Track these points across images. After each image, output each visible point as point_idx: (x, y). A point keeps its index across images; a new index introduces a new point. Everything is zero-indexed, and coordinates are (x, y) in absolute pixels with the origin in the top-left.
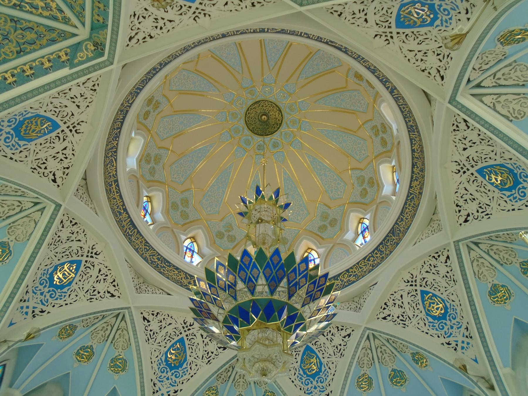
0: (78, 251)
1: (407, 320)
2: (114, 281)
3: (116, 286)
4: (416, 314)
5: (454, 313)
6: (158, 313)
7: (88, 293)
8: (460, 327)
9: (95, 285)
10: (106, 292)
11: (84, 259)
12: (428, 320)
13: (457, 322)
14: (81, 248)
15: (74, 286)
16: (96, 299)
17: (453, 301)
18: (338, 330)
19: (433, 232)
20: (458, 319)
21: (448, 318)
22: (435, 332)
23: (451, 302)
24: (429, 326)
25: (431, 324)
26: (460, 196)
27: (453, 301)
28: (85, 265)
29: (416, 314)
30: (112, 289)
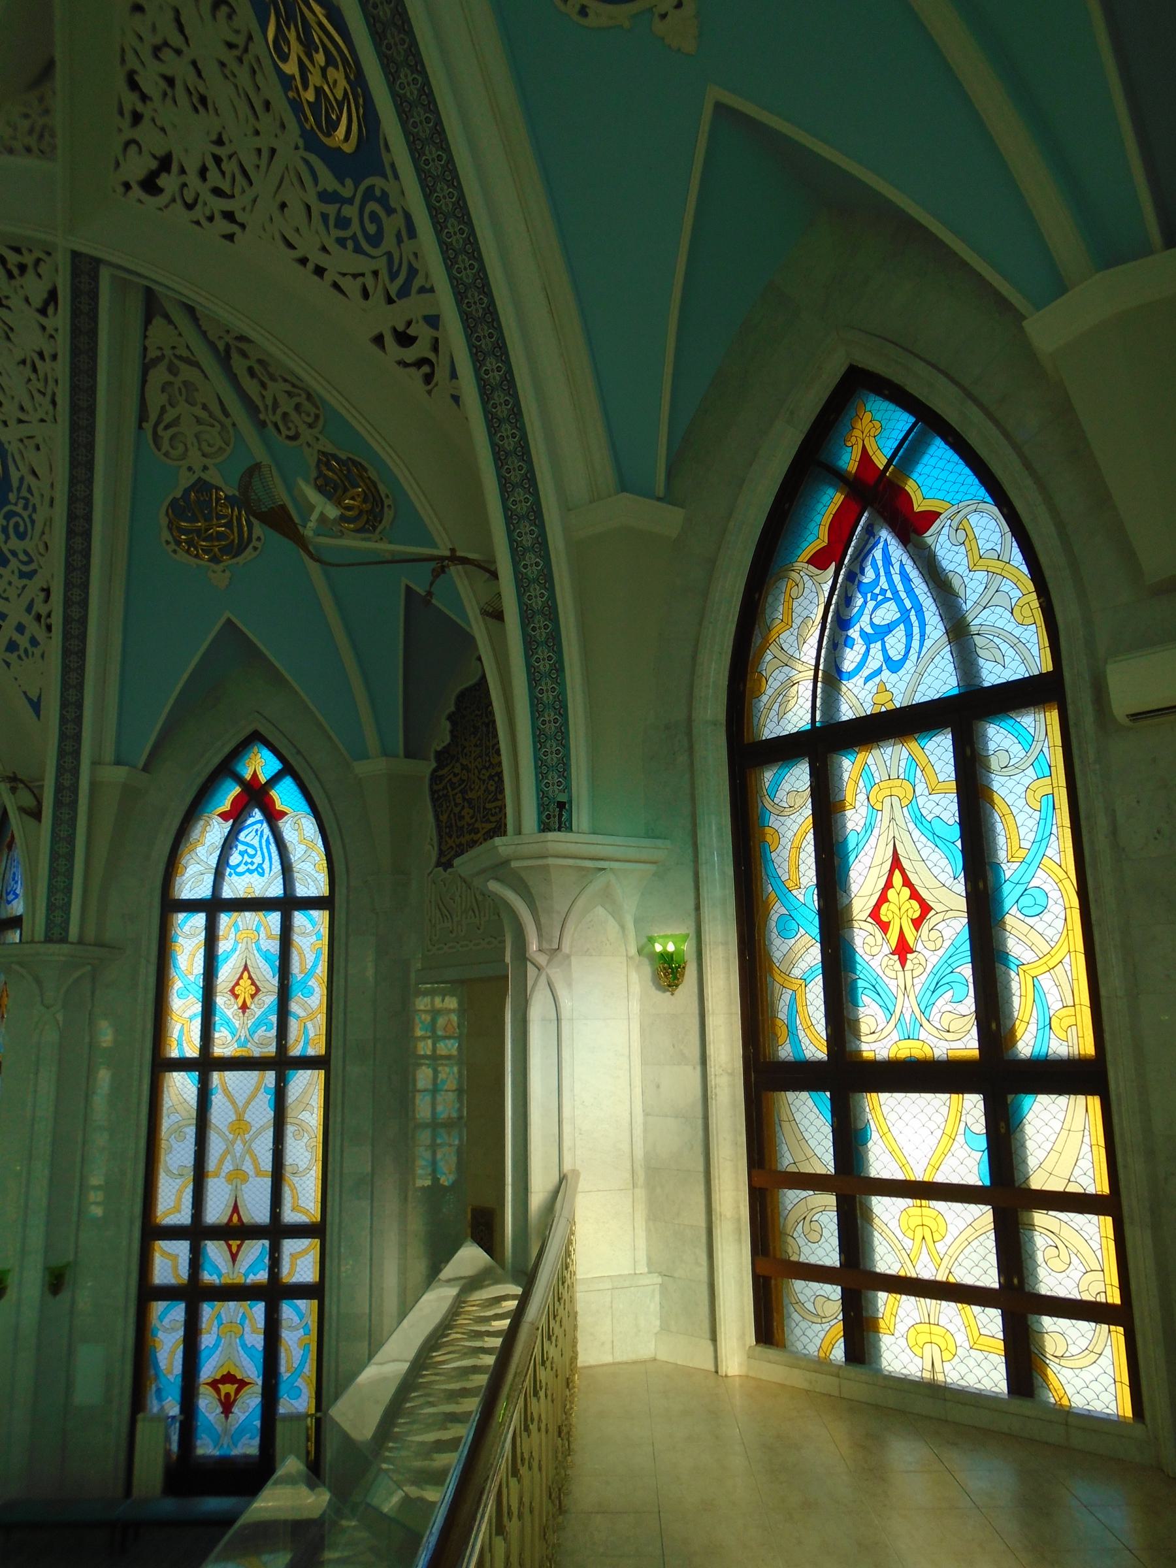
5: (25, 514)
8: (30, 575)
13: (26, 553)
23: (24, 470)
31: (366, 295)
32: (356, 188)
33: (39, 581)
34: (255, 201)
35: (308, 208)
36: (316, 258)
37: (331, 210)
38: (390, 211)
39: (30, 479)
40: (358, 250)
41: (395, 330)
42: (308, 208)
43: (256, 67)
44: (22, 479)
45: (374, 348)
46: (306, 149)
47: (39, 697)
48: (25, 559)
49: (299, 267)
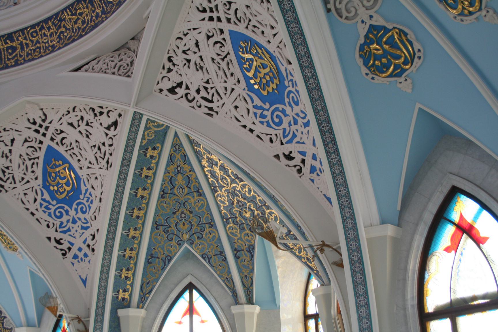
1: (9, 181)
4: (26, 178)
5: (87, 204)
8: (86, 228)
12: (42, 195)
13: (85, 219)
17: (93, 187)
19: (116, 70)
20: (87, 216)
21: (74, 206)
22: (46, 217)
23: (89, 186)
24: (41, 205)
25: (45, 204)
26: (182, 48)
27: (93, 187)
29: (26, 178)
31: (271, 141)
32: (270, 107)
33: (90, 231)
34: (223, 104)
35: (248, 110)
36: (250, 126)
37: (259, 112)
38: (286, 115)
39: (91, 190)
40: (269, 125)
41: (284, 154)
42: (248, 110)
43: (230, 62)
45: (275, 160)
46: (248, 90)
47: (86, 279)
48: (85, 222)
49: (243, 129)
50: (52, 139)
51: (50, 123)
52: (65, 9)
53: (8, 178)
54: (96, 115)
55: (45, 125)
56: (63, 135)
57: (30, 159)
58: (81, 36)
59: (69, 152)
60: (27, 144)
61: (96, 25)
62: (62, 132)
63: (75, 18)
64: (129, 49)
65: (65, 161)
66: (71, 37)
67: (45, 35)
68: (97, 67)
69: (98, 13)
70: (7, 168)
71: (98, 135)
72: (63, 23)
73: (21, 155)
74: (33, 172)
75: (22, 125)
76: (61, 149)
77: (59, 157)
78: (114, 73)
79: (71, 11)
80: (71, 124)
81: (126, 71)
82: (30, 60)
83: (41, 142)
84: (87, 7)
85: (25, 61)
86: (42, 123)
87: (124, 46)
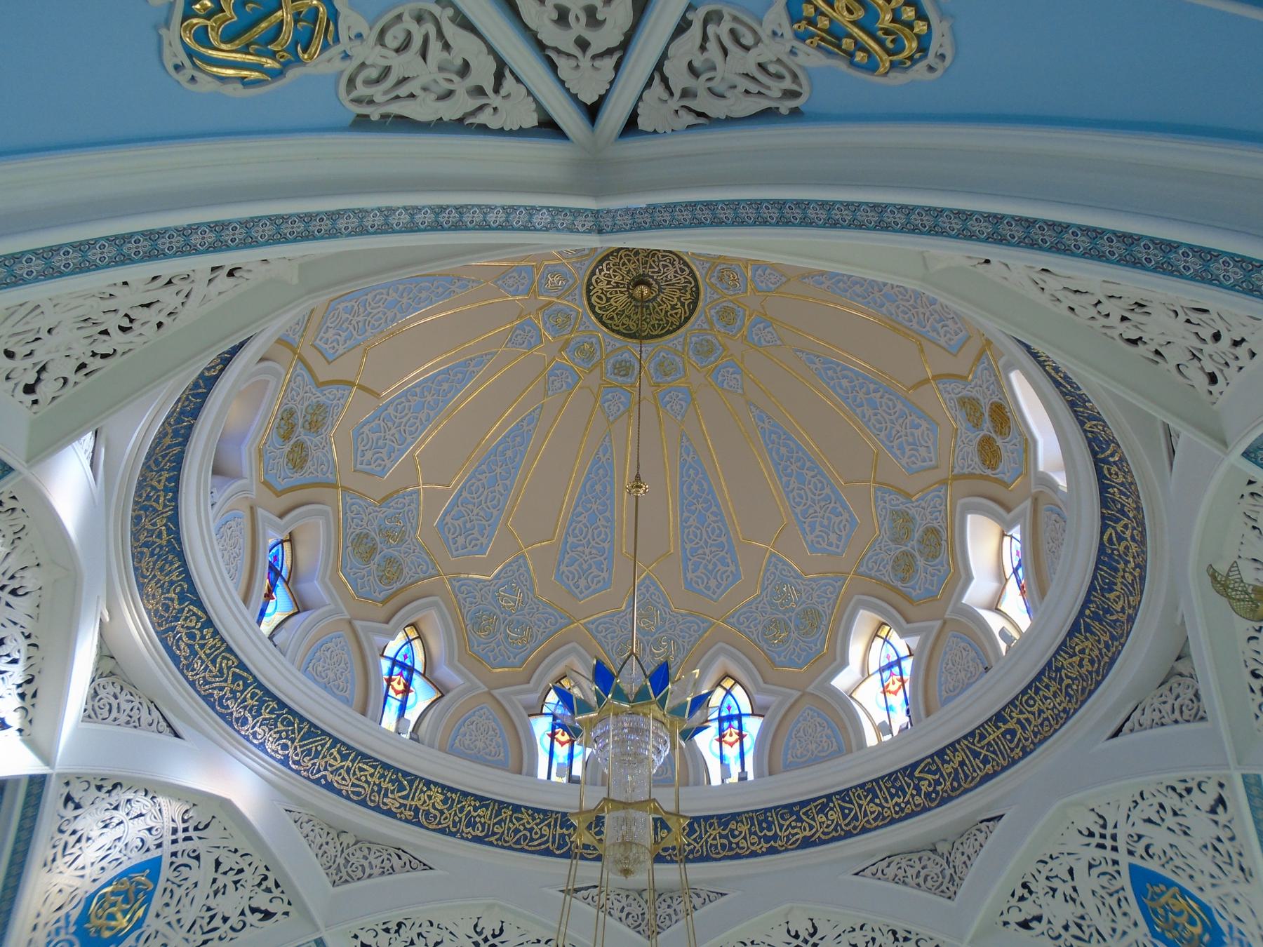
0: (142, 840)
1: (1094, 940)
2: (265, 878)
3: (273, 888)
6: (400, 925)
7: (197, 927)
9: (212, 902)
10: (247, 912)
11: (168, 848)
14: (150, 830)
15: (152, 924)
16: (221, 939)
17: (1239, 919)
18: (896, 940)
19: (1177, 715)
28: (172, 863)
30: (262, 901)
39: (1236, 923)
44: (1230, 927)
50: (1131, 853)
51: (1115, 827)
52: (1057, 652)
53: (1091, 935)
54: (1181, 796)
55: (1109, 831)
56: (1144, 842)
57: (1111, 895)
58: (1098, 683)
59: (1169, 866)
60: (1095, 871)
61: (1113, 661)
62: (1140, 837)
63: (1076, 659)
64: (1181, 675)
65: (1169, 884)
66: (1084, 689)
67: (1046, 698)
68: (1146, 720)
69: (1106, 643)
70: (1082, 918)
71: (1203, 828)
72: (1063, 672)
73: (1094, 893)
74: (1125, 914)
75: (1076, 842)
76: (1152, 865)
77: (1156, 879)
78: (1176, 722)
79: (1066, 653)
80: (1149, 821)
81: (1194, 711)
82: (1041, 742)
83: (1115, 862)
84: (1087, 639)
85: (1036, 745)
86: (1103, 831)
87: (1172, 673)
